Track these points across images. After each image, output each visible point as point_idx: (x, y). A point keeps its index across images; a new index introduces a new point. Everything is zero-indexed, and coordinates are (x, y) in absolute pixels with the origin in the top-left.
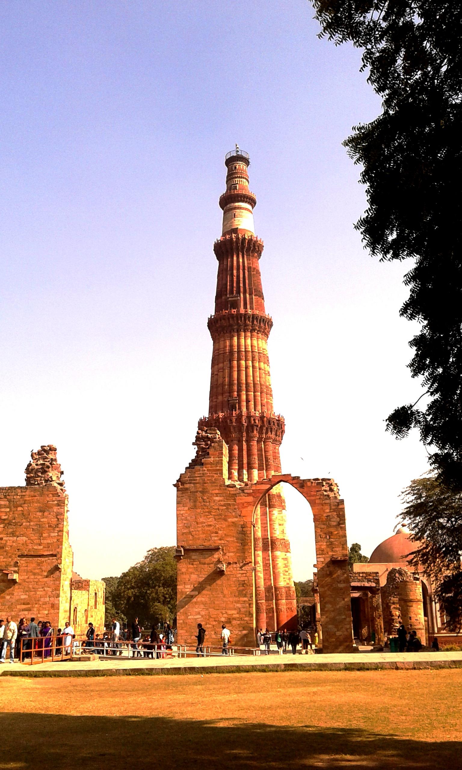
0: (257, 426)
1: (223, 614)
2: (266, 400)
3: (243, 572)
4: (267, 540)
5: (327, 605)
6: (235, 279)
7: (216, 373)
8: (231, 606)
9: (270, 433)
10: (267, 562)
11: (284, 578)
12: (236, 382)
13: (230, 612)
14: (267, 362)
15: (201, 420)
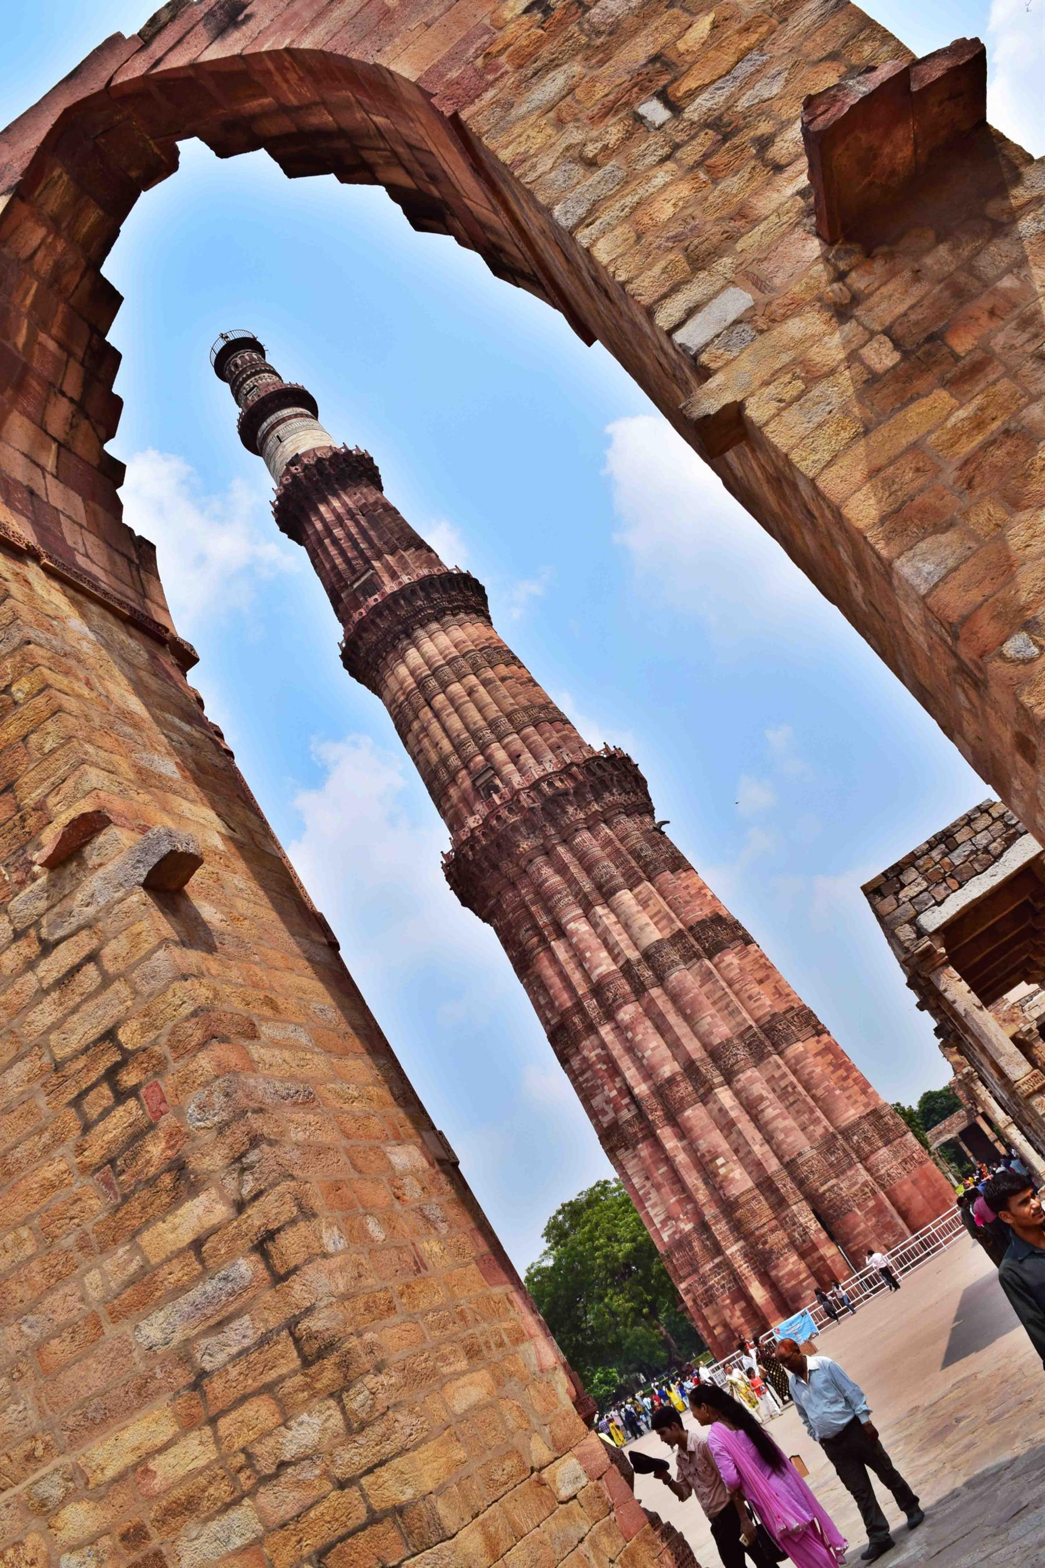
0: (565, 793)
1: (43, 1510)
2: (555, 734)
3: (64, 957)
6: (345, 544)
7: (416, 750)
8: (91, 1377)
9: (606, 795)
10: (783, 1084)
11: (849, 1098)
12: (465, 735)
13: (108, 1454)
15: (445, 867)
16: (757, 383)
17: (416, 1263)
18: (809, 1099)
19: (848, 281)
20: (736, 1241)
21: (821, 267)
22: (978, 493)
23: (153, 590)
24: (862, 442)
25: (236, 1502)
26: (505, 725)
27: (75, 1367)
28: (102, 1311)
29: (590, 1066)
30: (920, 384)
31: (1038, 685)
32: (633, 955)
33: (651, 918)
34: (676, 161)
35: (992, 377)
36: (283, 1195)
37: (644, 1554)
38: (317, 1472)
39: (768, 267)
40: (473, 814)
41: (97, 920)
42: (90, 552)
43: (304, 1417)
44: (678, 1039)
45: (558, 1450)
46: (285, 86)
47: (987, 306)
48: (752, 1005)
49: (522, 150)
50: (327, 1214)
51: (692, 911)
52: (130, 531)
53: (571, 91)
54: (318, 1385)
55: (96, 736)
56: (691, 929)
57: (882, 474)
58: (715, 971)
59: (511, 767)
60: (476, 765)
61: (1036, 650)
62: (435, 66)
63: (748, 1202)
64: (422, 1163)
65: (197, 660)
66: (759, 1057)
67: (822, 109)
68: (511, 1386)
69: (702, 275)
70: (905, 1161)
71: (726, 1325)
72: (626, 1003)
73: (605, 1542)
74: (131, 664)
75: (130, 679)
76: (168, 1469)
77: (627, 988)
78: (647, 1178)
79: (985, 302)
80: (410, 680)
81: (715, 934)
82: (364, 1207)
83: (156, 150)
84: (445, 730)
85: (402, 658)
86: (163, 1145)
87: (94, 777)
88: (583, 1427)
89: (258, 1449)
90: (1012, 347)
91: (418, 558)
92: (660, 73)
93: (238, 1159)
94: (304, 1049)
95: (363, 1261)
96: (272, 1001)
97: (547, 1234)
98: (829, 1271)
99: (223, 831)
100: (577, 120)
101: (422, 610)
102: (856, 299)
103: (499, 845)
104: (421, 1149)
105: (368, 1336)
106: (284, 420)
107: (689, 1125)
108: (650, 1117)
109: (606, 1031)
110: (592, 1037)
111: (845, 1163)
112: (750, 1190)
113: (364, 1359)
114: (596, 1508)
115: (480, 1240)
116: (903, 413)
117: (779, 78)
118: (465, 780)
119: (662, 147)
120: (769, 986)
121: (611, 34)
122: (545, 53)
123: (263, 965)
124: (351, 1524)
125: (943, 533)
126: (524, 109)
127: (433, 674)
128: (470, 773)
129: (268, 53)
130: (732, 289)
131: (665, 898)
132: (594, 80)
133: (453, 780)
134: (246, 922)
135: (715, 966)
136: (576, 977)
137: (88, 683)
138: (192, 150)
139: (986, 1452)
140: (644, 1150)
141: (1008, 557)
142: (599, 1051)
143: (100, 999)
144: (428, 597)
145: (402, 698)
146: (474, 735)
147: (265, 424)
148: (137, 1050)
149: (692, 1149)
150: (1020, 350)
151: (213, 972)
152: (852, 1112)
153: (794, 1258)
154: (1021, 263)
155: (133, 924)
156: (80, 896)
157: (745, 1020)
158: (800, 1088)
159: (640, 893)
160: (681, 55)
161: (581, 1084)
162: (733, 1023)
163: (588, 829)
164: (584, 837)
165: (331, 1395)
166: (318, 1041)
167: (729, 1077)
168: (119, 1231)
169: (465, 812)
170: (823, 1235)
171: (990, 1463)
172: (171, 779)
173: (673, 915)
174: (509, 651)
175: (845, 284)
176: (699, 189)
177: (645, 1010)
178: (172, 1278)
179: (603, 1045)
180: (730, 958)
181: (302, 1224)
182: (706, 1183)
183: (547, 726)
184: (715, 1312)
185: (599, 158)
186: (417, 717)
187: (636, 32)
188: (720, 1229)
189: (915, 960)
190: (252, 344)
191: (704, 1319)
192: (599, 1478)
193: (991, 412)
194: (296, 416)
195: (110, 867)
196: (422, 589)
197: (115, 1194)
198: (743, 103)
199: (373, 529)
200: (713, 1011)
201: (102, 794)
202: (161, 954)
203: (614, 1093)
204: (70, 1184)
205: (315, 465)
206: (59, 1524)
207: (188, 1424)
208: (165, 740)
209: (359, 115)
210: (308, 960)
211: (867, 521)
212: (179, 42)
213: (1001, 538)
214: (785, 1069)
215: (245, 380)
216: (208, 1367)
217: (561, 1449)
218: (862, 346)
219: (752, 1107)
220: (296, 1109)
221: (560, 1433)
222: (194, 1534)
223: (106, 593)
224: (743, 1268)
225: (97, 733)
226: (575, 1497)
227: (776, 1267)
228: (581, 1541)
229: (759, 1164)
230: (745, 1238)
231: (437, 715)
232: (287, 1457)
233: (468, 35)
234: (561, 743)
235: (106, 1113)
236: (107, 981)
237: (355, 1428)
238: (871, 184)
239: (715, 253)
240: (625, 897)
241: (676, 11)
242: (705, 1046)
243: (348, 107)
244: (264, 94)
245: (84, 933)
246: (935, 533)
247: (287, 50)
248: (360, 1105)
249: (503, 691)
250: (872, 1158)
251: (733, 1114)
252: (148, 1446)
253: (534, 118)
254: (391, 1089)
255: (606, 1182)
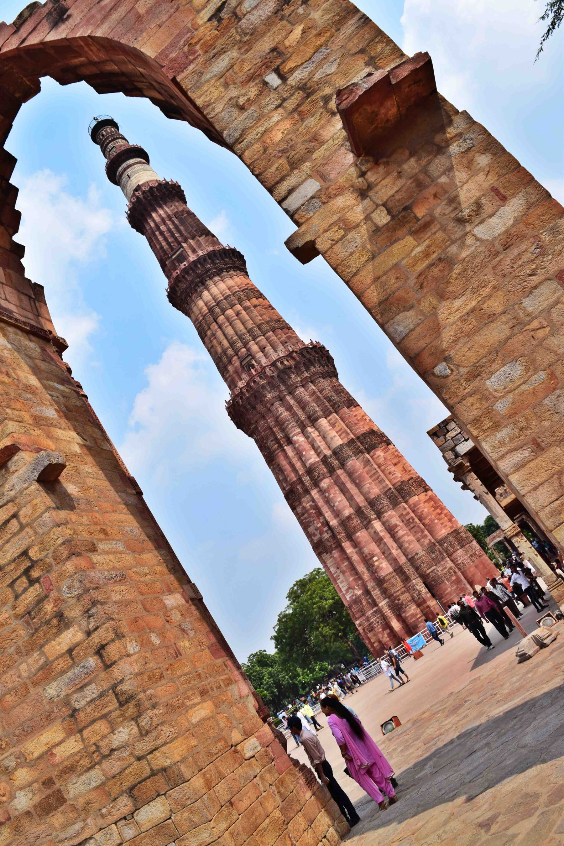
0: (290, 368)
2: (284, 336)
4: (390, 491)
5: (492, 383)
6: (167, 234)
7: (210, 346)
8: (25, 712)
9: (312, 368)
10: (407, 518)
11: (442, 524)
13: (35, 746)
14: (260, 295)
16: (321, 231)
17: (176, 653)
18: (421, 525)
19: (366, 177)
20: (385, 599)
21: (353, 169)
22: (425, 291)
23: (43, 311)
24: (371, 263)
25: (93, 767)
26: (257, 331)
27: (17, 708)
28: (28, 681)
29: (307, 511)
30: (399, 233)
31: (449, 389)
32: (328, 452)
33: (337, 432)
34: (284, 108)
35: (434, 230)
36: (107, 629)
37: (289, 780)
38: (128, 753)
39: (328, 168)
40: (241, 380)
41: (16, 498)
42: (8, 297)
43: (121, 729)
44: (352, 496)
45: (246, 735)
46: (91, 53)
47: (433, 192)
48: (391, 477)
49: (207, 99)
50: (130, 635)
51: (359, 428)
52: (30, 281)
53: (232, 67)
54: (127, 715)
55: (12, 404)
56: (358, 438)
57: (380, 280)
58: (371, 460)
59: (261, 354)
60: (242, 353)
61: (449, 371)
62: (164, 50)
63: (390, 579)
64: (182, 601)
65: (67, 347)
66: (395, 504)
67: (345, 97)
68: (224, 707)
69: (296, 172)
70: (471, 556)
71: (380, 642)
72: (324, 478)
73: (268, 776)
74: (30, 357)
75: (30, 366)
76: (62, 753)
77: (325, 470)
78: (338, 568)
79: (432, 190)
80: (205, 308)
81: (373, 440)
82: (150, 629)
83: (28, 83)
84: (225, 335)
85: (200, 296)
86: (52, 605)
87: (11, 426)
88: (260, 721)
89: (101, 744)
90: (444, 214)
91: (207, 241)
92: (276, 58)
93: (87, 612)
94: (121, 553)
95: (148, 656)
96: (104, 530)
97: (289, 596)
98: (432, 613)
99: (80, 442)
100: (235, 83)
101: (210, 270)
102: (370, 187)
103: (255, 396)
104: (182, 594)
105: (149, 692)
106: (130, 166)
107: (359, 540)
108: (339, 537)
109: (314, 493)
110: (308, 496)
111: (440, 557)
112: (390, 573)
113: (146, 703)
114: (264, 761)
115: (212, 637)
116: (391, 248)
117: (335, 63)
118: (236, 362)
119: (277, 100)
120: (400, 466)
121: (252, 34)
122: (219, 45)
123: (100, 512)
124: (144, 776)
125: (408, 311)
126: (208, 76)
127: (217, 305)
128: (239, 358)
129: (80, 38)
130: (310, 180)
131: (344, 422)
132: (243, 61)
133: (230, 362)
134: (92, 490)
135: (371, 457)
136: (298, 465)
137: (8, 374)
138: (47, 83)
139: (470, 721)
140: (336, 554)
141: (438, 324)
142: (311, 503)
143: (20, 536)
144: (213, 262)
145: (201, 318)
146: (240, 337)
147: (120, 169)
148: (38, 560)
149: (360, 553)
150: (448, 216)
151: (74, 520)
152: (444, 531)
153: (414, 607)
154: (450, 169)
155: (33, 500)
156: (7, 486)
157: (387, 485)
158: (416, 520)
159: (331, 419)
160: (286, 48)
161: (302, 520)
162: (381, 487)
163: (303, 386)
164: (300, 391)
165: (133, 719)
166: (128, 547)
167: (379, 516)
168: (34, 645)
169: (237, 378)
170: (429, 595)
171: (470, 727)
172: (52, 419)
173: (349, 431)
174: (258, 291)
175: (365, 179)
176: (294, 124)
177: (335, 481)
178: (60, 667)
179: (313, 500)
180: (379, 453)
181: (117, 642)
182: (368, 570)
183: (279, 331)
184: (374, 635)
185: (246, 105)
186: (210, 328)
187: (264, 34)
188: (376, 593)
189: (454, 469)
190: (111, 123)
191: (369, 639)
192: (268, 746)
193: (433, 248)
194: (137, 163)
195: (21, 472)
196: (210, 258)
197: (32, 628)
198: (317, 77)
199: (182, 225)
200: (370, 481)
201: (15, 435)
202: (47, 514)
203: (320, 525)
204: (10, 624)
205: (149, 191)
206: (15, 778)
207: (70, 733)
208: (49, 397)
209: (131, 67)
210: (125, 504)
211: (373, 304)
212: (34, 29)
213: (435, 315)
214: (408, 510)
215: (108, 143)
216: (77, 707)
217: (247, 734)
218: (372, 212)
219: (391, 530)
220: (115, 585)
221: (248, 727)
222: (75, 781)
223: (16, 320)
224: (388, 613)
225: (13, 402)
226: (254, 756)
227: (404, 612)
228: (255, 777)
229: (395, 560)
230: (389, 598)
231: (220, 327)
232: (114, 747)
233: (180, 33)
234: (287, 340)
235: (25, 590)
236: (22, 527)
237: (143, 733)
238: (376, 128)
239: (302, 160)
240: (323, 422)
241: (284, 22)
242: (366, 499)
243: (124, 63)
244: (80, 56)
245: (10, 504)
246: (404, 311)
247: (89, 36)
248: (149, 577)
249: (255, 313)
250: (454, 555)
251: (381, 534)
252: (52, 742)
253: (213, 81)
254: (167, 565)
255: (319, 569)
